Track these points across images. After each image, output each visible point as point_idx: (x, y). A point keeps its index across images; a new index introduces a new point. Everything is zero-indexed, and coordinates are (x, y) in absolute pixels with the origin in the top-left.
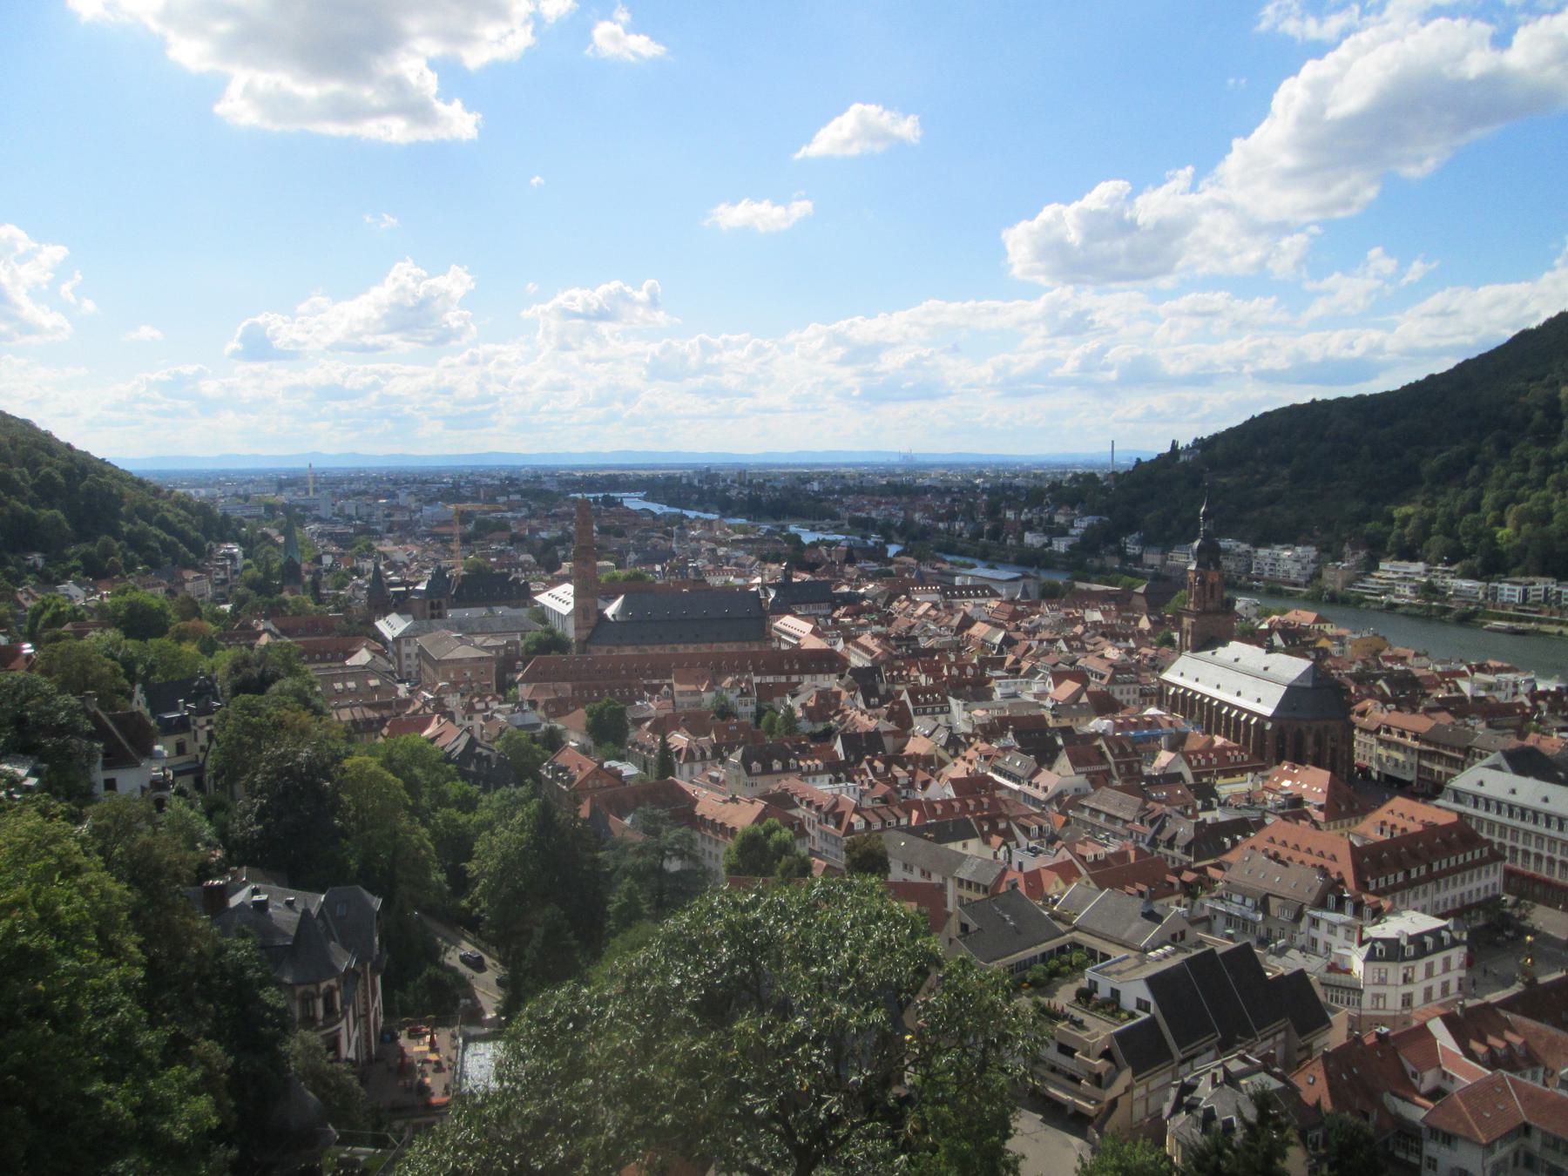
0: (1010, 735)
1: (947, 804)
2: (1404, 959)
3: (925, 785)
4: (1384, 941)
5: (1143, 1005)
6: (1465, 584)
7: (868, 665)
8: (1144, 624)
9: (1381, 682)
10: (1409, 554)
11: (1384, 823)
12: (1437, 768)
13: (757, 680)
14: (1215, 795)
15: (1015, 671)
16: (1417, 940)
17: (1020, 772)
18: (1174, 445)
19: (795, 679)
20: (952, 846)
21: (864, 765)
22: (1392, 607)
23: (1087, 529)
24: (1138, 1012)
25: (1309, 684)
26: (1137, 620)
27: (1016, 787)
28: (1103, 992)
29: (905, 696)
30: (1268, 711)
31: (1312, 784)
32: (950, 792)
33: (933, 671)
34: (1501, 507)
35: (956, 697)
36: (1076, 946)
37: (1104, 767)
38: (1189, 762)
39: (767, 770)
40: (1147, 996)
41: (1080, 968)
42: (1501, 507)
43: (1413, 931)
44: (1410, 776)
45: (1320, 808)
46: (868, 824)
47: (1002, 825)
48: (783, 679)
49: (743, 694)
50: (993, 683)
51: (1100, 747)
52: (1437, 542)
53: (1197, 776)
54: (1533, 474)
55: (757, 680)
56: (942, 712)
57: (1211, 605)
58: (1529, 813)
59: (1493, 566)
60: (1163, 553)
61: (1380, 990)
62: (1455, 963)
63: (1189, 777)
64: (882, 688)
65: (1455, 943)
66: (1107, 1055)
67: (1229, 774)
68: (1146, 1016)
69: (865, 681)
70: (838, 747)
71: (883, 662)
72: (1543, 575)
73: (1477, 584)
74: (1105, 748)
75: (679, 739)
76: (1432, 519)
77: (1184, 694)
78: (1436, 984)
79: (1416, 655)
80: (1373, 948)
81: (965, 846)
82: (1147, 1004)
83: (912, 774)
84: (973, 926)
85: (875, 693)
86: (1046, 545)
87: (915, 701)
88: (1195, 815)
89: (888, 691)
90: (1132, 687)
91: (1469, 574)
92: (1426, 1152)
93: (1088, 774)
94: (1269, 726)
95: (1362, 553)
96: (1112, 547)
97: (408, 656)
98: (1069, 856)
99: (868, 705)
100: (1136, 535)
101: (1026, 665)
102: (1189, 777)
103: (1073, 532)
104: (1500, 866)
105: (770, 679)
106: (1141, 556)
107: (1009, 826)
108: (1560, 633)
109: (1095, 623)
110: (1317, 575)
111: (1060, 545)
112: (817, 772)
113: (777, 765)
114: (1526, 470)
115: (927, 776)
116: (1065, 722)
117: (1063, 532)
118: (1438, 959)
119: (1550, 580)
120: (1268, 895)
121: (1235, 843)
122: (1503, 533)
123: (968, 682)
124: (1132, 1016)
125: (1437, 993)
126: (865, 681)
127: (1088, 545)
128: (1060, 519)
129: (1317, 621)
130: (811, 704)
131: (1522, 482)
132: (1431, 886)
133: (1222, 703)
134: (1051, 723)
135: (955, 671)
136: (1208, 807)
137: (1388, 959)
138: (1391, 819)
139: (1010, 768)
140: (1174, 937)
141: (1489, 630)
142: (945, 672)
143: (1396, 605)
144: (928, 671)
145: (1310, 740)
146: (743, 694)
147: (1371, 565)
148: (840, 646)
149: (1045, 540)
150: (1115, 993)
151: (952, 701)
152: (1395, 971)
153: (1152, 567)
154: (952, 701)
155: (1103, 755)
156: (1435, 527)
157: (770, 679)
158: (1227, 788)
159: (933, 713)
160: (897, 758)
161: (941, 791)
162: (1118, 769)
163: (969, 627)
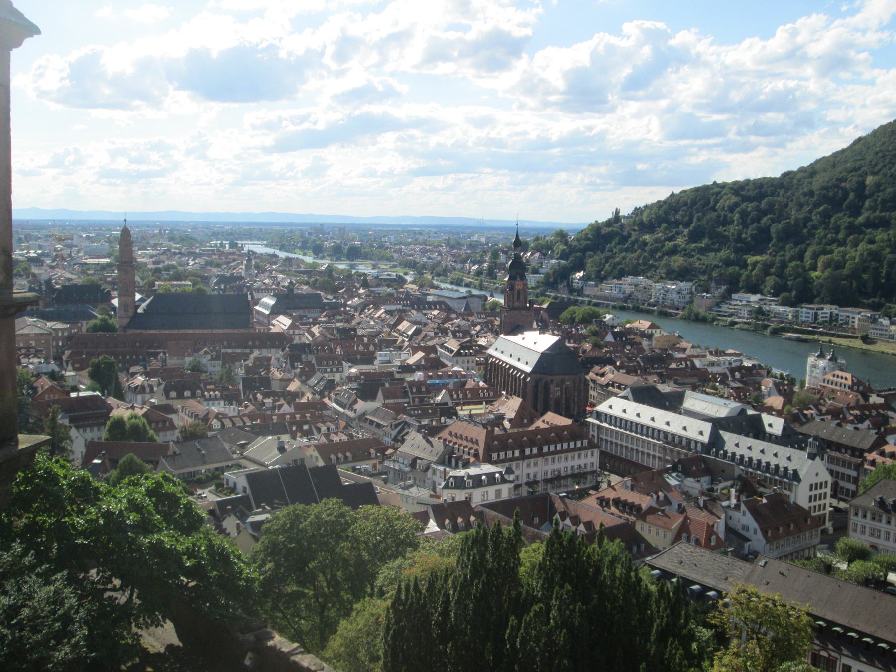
2: (465, 488)
6: (781, 309)
10: (754, 289)
17: (345, 401)
18: (617, 212)
22: (733, 323)
27: (341, 410)
30: (528, 369)
34: (815, 256)
42: (815, 256)
46: (223, 425)
49: (212, 359)
52: (770, 281)
54: (841, 236)
56: (337, 371)
57: (517, 304)
58: (656, 433)
59: (804, 294)
72: (832, 304)
73: (788, 309)
76: (772, 265)
79: (693, 347)
91: (783, 304)
94: (528, 379)
95: (724, 288)
100: (581, 274)
108: (830, 342)
110: (691, 302)
112: (216, 399)
114: (837, 233)
119: (834, 307)
120: (417, 458)
122: (814, 274)
129: (650, 327)
131: (833, 241)
132: (539, 460)
133: (511, 367)
135: (361, 348)
141: (785, 339)
143: (736, 323)
146: (212, 359)
147: (726, 297)
153: (588, 296)
156: (773, 270)
159: (331, 372)
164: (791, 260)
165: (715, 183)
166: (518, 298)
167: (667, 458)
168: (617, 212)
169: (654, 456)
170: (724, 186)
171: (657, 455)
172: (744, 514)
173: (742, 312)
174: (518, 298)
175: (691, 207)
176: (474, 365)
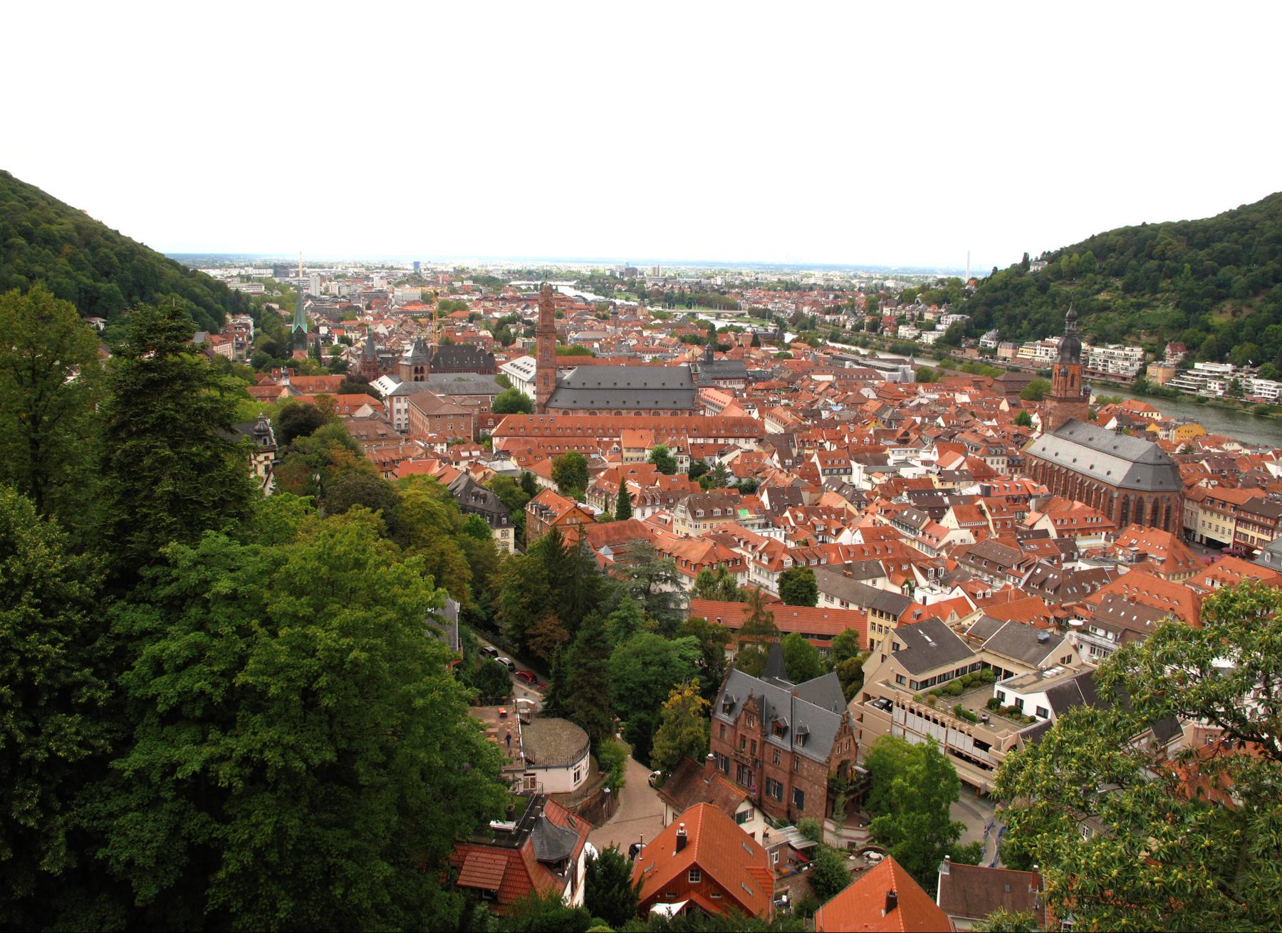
0: (905, 494)
1: (860, 549)
3: (839, 531)
5: (1042, 712)
7: (782, 431)
8: (1004, 406)
9: (1203, 462)
13: (690, 441)
14: (1076, 549)
15: (904, 441)
18: (1026, 256)
19: (721, 441)
20: (864, 582)
21: (787, 514)
22: (1202, 401)
23: (954, 324)
24: (1038, 718)
25: (1151, 460)
26: (998, 404)
28: (1009, 702)
29: (815, 459)
31: (1157, 543)
32: (858, 539)
33: (838, 439)
35: (858, 461)
36: (986, 665)
37: (984, 523)
38: (1054, 522)
39: (709, 515)
40: (1046, 704)
41: (991, 683)
44: (1228, 540)
45: (1162, 562)
47: (905, 568)
48: (711, 441)
50: (888, 451)
51: (980, 506)
53: (1060, 533)
55: (690, 441)
56: (845, 473)
57: (1070, 394)
60: (1014, 348)
63: (1053, 534)
64: (795, 452)
67: (1086, 532)
69: (782, 444)
70: (765, 498)
71: (795, 430)
74: (984, 507)
75: (633, 486)
76: (1240, 326)
77: (1044, 466)
81: (874, 582)
82: (1046, 711)
83: (827, 523)
84: (903, 646)
85: (790, 456)
86: (916, 338)
87: (823, 463)
88: (1060, 565)
89: (799, 455)
90: (1001, 459)
93: (971, 528)
96: (972, 341)
97: (399, 411)
98: (962, 594)
99: (783, 464)
101: (913, 436)
102: (1053, 534)
103: (939, 327)
105: (700, 441)
106: (996, 349)
107: (910, 569)
109: (964, 404)
110: (1143, 371)
111: (929, 338)
113: (717, 511)
115: (839, 525)
116: (949, 485)
117: (932, 328)
121: (1094, 588)
123: (866, 450)
124: (1033, 720)
126: (782, 444)
127: (953, 339)
128: (928, 316)
130: (737, 462)
134: (937, 485)
135: (854, 440)
136: (1070, 558)
139: (907, 520)
140: (1063, 660)
142: (846, 440)
144: (832, 440)
145: (1148, 508)
148: (755, 415)
149: (916, 333)
150: (1020, 703)
151: (853, 463)
153: (1005, 359)
154: (854, 465)
155: (983, 513)
157: (700, 441)
158: (1083, 543)
159: (838, 473)
160: (813, 509)
161: (851, 538)
162: (995, 525)
163: (862, 404)
164: (1267, 322)
165: (1144, 224)
166: (1072, 385)
168: (1026, 256)
170: (1155, 228)
173: (1212, 385)
174: (1072, 385)
175: (1122, 254)
176: (1004, 466)
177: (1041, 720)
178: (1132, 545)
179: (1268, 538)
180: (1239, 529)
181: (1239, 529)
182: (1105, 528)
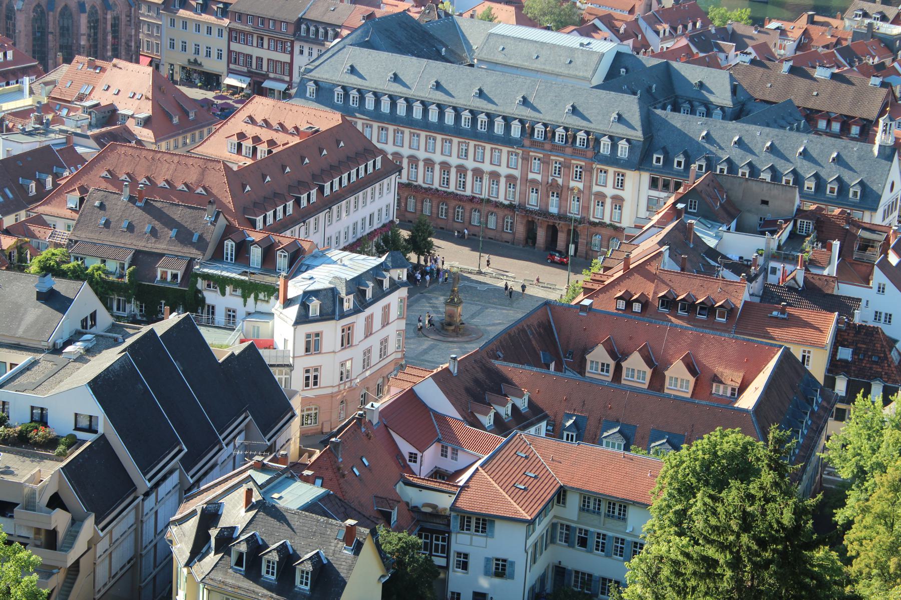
2: (343, 316)
4: (316, 293)
11: (241, 136)
12: (256, 52)
16: (356, 285)
24: (81, 435)
43: (351, 275)
61: (312, 361)
62: (394, 313)
65: (395, 286)
66: (56, 502)
68: (90, 438)
78: (374, 342)
80: (305, 307)
92: (455, 547)
104: (392, 181)
118: (376, 310)
121: (41, 184)
124: (74, 442)
125: (375, 357)
137: (325, 316)
138: (251, 131)
152: (331, 331)
167: (531, 176)
169: (495, 176)
171: (503, 171)
172: (881, 289)
177: (90, 438)
178: (81, 98)
179: (286, 58)
180: (235, 46)
181: (235, 46)
182: (25, 72)
